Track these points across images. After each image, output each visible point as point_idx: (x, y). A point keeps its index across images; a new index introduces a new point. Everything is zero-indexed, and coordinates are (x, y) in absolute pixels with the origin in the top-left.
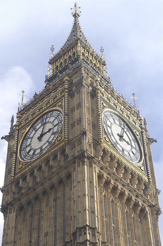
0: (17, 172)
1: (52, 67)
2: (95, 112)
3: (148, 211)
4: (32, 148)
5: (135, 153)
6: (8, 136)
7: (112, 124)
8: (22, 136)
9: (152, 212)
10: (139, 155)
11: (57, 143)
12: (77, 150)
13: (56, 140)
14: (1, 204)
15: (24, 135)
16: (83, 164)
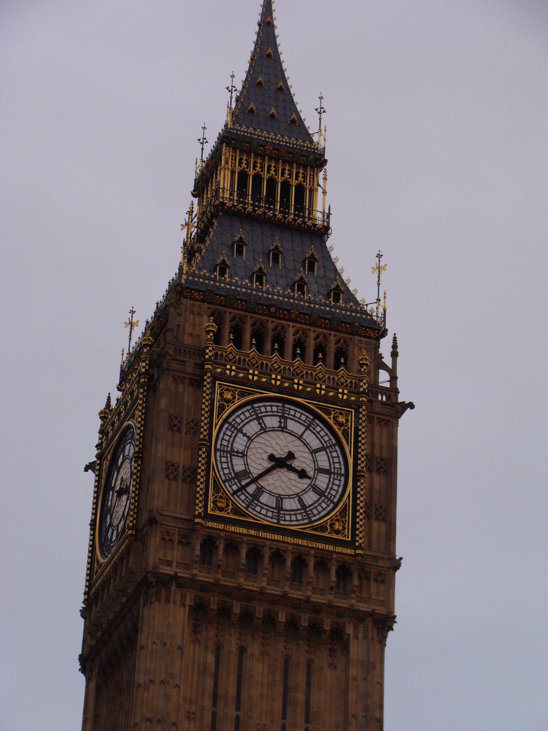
7: (252, 438)
16: (151, 603)
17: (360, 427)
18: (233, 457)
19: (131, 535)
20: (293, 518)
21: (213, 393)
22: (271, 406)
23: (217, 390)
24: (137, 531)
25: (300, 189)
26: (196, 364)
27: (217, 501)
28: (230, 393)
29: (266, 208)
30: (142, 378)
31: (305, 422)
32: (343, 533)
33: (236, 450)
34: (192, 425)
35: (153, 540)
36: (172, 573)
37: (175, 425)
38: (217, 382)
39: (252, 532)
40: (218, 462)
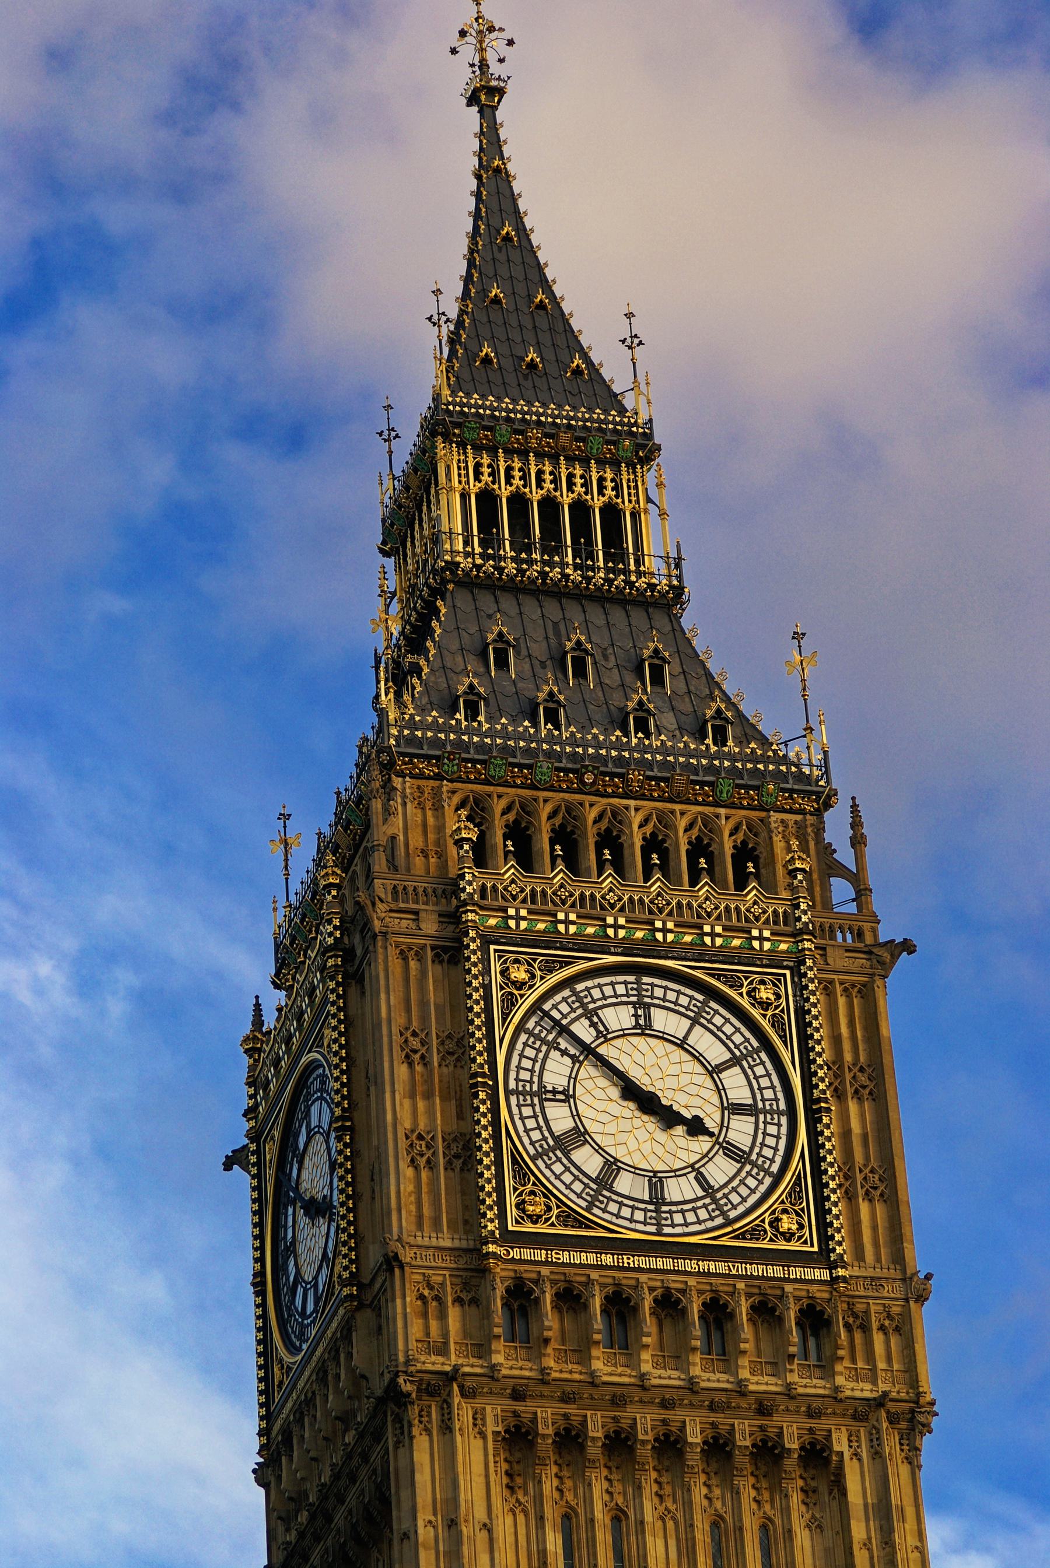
17: (807, 1006)
18: (546, 1104)
19: (350, 1297)
20: (691, 1217)
21: (487, 971)
22: (612, 984)
23: (496, 967)
24: (361, 1286)
25: (612, 514)
26: (440, 915)
27: (524, 1202)
28: (522, 968)
29: (544, 563)
30: (330, 957)
31: (687, 1008)
32: (800, 1238)
33: (549, 1088)
34: (450, 1045)
36: (448, 1368)
37: (415, 1051)
38: (492, 947)
39: (608, 1259)
40: (517, 1118)
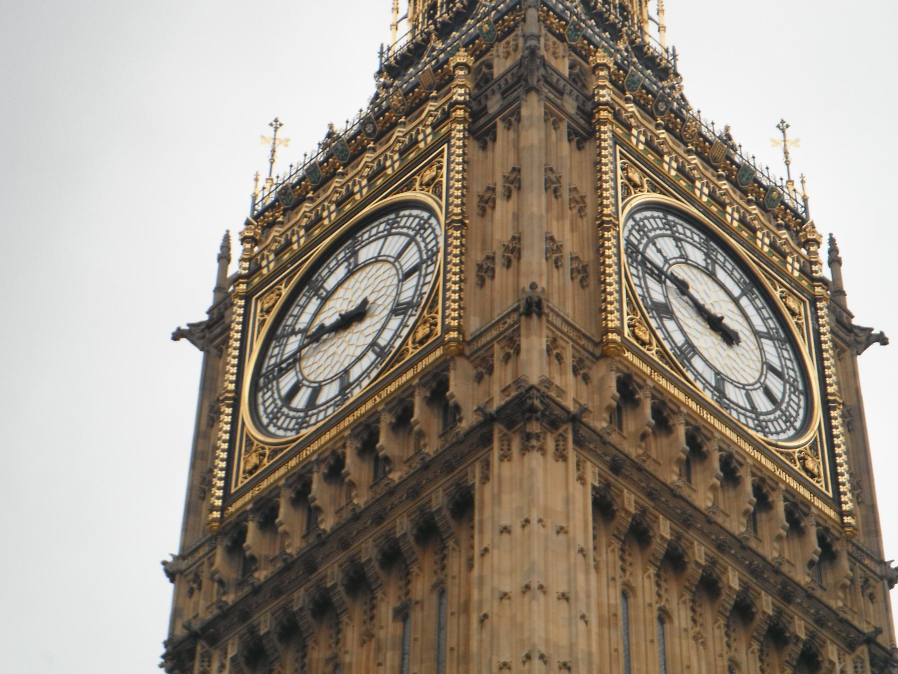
0: (236, 485)
1: (411, 9)
2: (589, 211)
3: (836, 660)
4: (304, 378)
5: (778, 395)
6: (203, 327)
7: (671, 262)
8: (262, 323)
9: (859, 665)
10: (798, 405)
11: (412, 351)
12: (500, 380)
13: (410, 341)
14: (165, 636)
15: (270, 319)
16: (525, 449)
30: (460, 109)
35: (534, 338)
38: (618, 148)
